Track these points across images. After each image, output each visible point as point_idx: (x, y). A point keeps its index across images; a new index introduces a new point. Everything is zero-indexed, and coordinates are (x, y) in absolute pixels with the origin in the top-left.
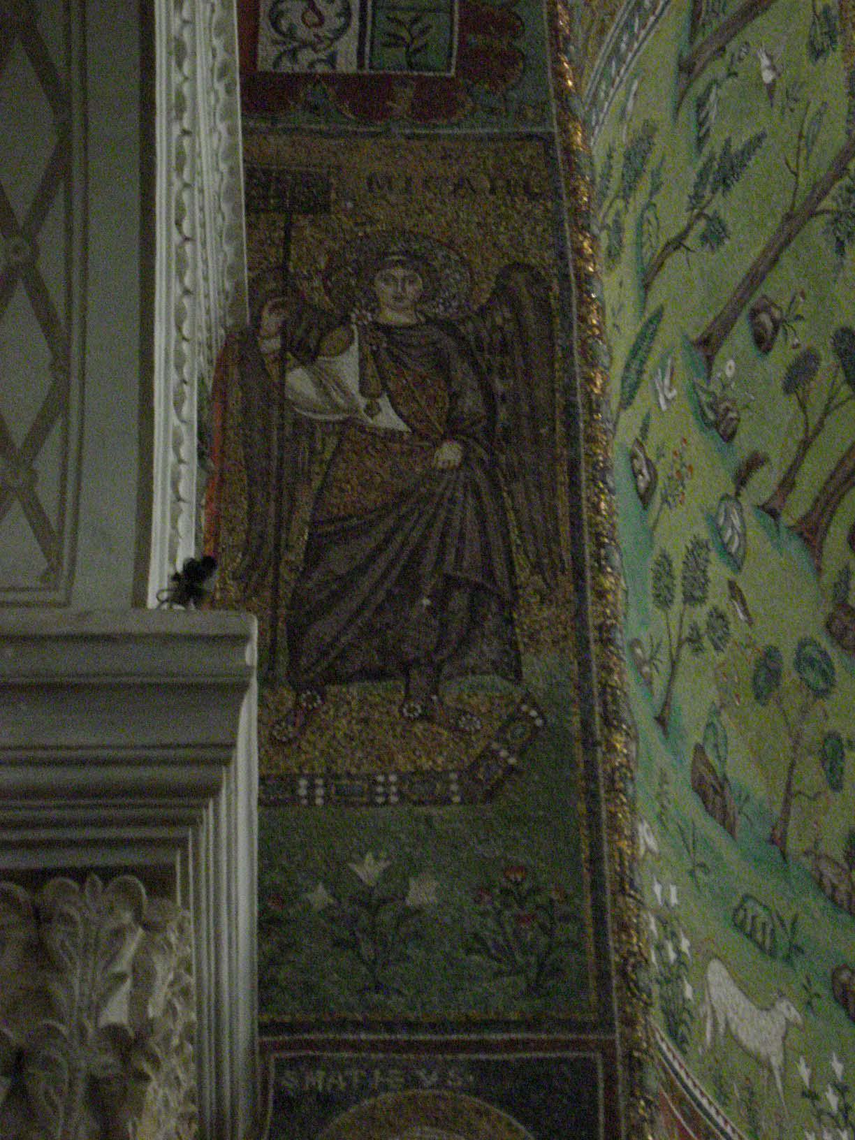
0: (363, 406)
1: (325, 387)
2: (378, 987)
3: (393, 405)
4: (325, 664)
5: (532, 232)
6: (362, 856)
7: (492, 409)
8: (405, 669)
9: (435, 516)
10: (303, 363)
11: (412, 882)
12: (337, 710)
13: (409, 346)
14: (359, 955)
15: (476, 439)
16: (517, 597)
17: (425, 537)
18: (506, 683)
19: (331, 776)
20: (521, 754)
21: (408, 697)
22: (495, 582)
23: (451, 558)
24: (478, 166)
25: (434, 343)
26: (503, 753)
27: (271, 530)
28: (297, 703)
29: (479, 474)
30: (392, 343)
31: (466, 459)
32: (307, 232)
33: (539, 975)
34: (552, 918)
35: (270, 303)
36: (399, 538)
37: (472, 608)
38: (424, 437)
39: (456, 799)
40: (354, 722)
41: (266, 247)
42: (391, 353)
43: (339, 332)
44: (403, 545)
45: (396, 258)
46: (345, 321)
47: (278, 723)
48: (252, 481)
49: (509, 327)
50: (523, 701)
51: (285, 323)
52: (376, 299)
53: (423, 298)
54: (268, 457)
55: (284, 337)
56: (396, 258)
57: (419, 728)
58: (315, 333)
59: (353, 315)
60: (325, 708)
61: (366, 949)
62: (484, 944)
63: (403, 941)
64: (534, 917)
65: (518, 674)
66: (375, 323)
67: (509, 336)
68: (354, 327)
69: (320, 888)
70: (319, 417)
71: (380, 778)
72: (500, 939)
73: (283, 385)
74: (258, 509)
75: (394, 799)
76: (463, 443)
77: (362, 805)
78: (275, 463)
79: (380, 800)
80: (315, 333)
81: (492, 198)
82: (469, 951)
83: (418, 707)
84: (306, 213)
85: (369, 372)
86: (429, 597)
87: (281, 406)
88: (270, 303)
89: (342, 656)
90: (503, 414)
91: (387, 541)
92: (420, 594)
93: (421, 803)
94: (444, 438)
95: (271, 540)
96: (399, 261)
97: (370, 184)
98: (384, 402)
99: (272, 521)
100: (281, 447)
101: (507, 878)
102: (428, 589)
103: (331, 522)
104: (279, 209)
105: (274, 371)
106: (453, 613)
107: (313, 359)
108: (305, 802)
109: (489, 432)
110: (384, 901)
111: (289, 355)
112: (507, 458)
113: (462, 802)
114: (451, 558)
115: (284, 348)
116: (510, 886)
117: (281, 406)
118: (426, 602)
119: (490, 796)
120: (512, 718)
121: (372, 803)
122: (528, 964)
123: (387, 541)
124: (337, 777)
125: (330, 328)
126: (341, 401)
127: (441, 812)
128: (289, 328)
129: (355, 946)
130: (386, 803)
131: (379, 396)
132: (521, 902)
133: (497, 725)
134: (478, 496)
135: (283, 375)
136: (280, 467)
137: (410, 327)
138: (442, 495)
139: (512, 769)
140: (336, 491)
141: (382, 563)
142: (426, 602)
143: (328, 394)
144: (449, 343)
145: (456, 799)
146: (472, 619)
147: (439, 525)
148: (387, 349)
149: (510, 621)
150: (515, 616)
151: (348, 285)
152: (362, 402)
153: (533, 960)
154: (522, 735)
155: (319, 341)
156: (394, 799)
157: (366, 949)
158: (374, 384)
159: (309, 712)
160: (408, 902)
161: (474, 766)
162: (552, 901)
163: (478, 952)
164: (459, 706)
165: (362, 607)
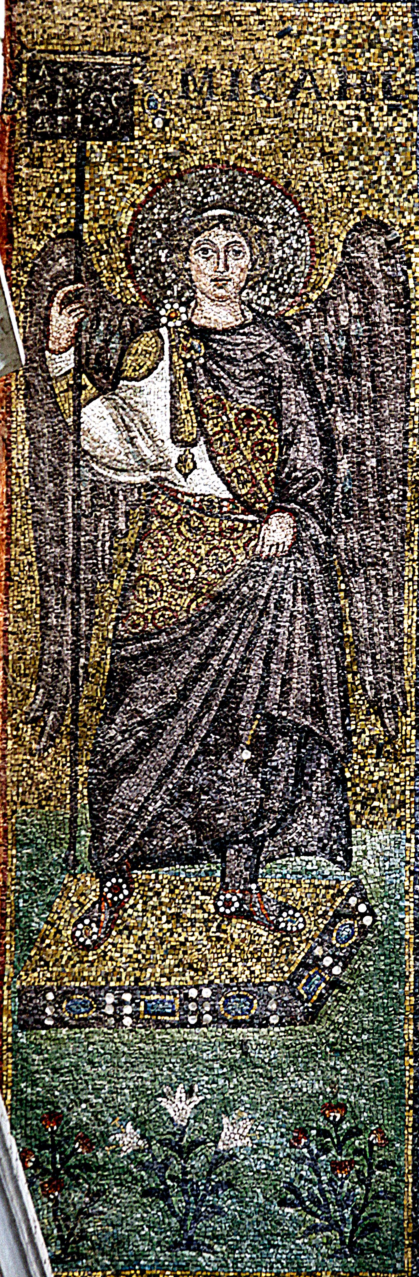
0: (175, 461)
1: (128, 429)
2: (190, 1244)
3: (211, 458)
4: (132, 841)
5: (390, 166)
6: (174, 1088)
7: (330, 461)
8: (221, 848)
9: (257, 631)
10: (102, 391)
11: (225, 1120)
12: (145, 903)
13: (231, 361)
14: (171, 1206)
15: (311, 509)
16: (350, 748)
17: (246, 661)
18: (334, 867)
19: (138, 988)
20: (346, 961)
21: (225, 887)
22: (326, 725)
23: (275, 692)
24: (324, 47)
25: (261, 356)
26: (328, 961)
27: (67, 652)
28: (102, 898)
29: (313, 566)
30: (211, 358)
31: (297, 538)
32: (105, 171)
33: (352, 1232)
34: (370, 1166)
35: (60, 294)
36: (215, 662)
37: (300, 764)
38: (249, 509)
39: (274, 1020)
40: (164, 918)
41: (54, 199)
42: (208, 372)
43: (146, 341)
44: (220, 673)
45: (217, 212)
46: (153, 323)
47: (81, 920)
48: (44, 576)
49: (357, 328)
50: (352, 892)
51: (78, 326)
52: (190, 286)
53: (252, 283)
54: (62, 542)
55: (78, 352)
56: (217, 212)
57: (236, 929)
58: (115, 345)
59: (163, 312)
60: (132, 902)
61: (178, 1202)
62: (298, 1196)
63: (214, 1191)
64: (352, 1163)
65: (348, 855)
66: (189, 323)
67: (355, 342)
68: (164, 331)
69: (129, 1127)
70: (123, 478)
71: (193, 993)
72: (316, 1192)
73: (77, 424)
74: (52, 621)
75: (208, 1018)
76: (292, 513)
77: (173, 1026)
78: (70, 553)
79: (192, 1020)
80: (115, 345)
81: (341, 105)
82: (283, 1203)
83: (234, 899)
84: (104, 136)
85: (183, 406)
86: (248, 747)
87: (76, 463)
88: (60, 294)
89: (149, 833)
90: (344, 466)
91: (203, 667)
92: (236, 742)
93: (236, 1024)
94: (272, 510)
95: (69, 665)
96: (222, 218)
97: (184, 82)
98: (200, 451)
99: (69, 638)
100: (77, 527)
101: (327, 1118)
102: (246, 735)
103: (138, 638)
104: (69, 130)
105: (67, 407)
106: (275, 768)
107: (115, 386)
108: (112, 1021)
109: (327, 499)
110: (195, 1144)
111: (85, 380)
112: (347, 541)
113: (280, 1024)
114: (275, 692)
115: (79, 368)
116: (330, 1128)
117: (76, 463)
118: (247, 755)
119: (311, 1017)
120: (338, 915)
121: (183, 1024)
122: (344, 1220)
123: (203, 667)
124: (147, 990)
125: (136, 333)
126: (148, 453)
127: (257, 1036)
128: (85, 338)
129: (165, 1196)
130: (199, 1024)
131: (194, 444)
132: (339, 1147)
133: (323, 923)
134: (309, 598)
135: (77, 412)
136: (76, 557)
137: (233, 331)
138: (269, 596)
139: (334, 984)
140: (142, 595)
141: (195, 702)
142: (247, 755)
143: (131, 440)
144: (281, 355)
145: (274, 1020)
146: (298, 779)
147: (262, 641)
148: (205, 364)
149: (341, 781)
150: (348, 775)
151: (158, 262)
152: (174, 452)
153: (347, 1213)
154: (350, 937)
155: (123, 353)
156: (208, 1018)
157: (178, 1202)
158: (190, 427)
159: (114, 903)
160: (221, 1146)
161: (295, 978)
162: (371, 1144)
163: (292, 1205)
164: (280, 899)
165: (173, 763)
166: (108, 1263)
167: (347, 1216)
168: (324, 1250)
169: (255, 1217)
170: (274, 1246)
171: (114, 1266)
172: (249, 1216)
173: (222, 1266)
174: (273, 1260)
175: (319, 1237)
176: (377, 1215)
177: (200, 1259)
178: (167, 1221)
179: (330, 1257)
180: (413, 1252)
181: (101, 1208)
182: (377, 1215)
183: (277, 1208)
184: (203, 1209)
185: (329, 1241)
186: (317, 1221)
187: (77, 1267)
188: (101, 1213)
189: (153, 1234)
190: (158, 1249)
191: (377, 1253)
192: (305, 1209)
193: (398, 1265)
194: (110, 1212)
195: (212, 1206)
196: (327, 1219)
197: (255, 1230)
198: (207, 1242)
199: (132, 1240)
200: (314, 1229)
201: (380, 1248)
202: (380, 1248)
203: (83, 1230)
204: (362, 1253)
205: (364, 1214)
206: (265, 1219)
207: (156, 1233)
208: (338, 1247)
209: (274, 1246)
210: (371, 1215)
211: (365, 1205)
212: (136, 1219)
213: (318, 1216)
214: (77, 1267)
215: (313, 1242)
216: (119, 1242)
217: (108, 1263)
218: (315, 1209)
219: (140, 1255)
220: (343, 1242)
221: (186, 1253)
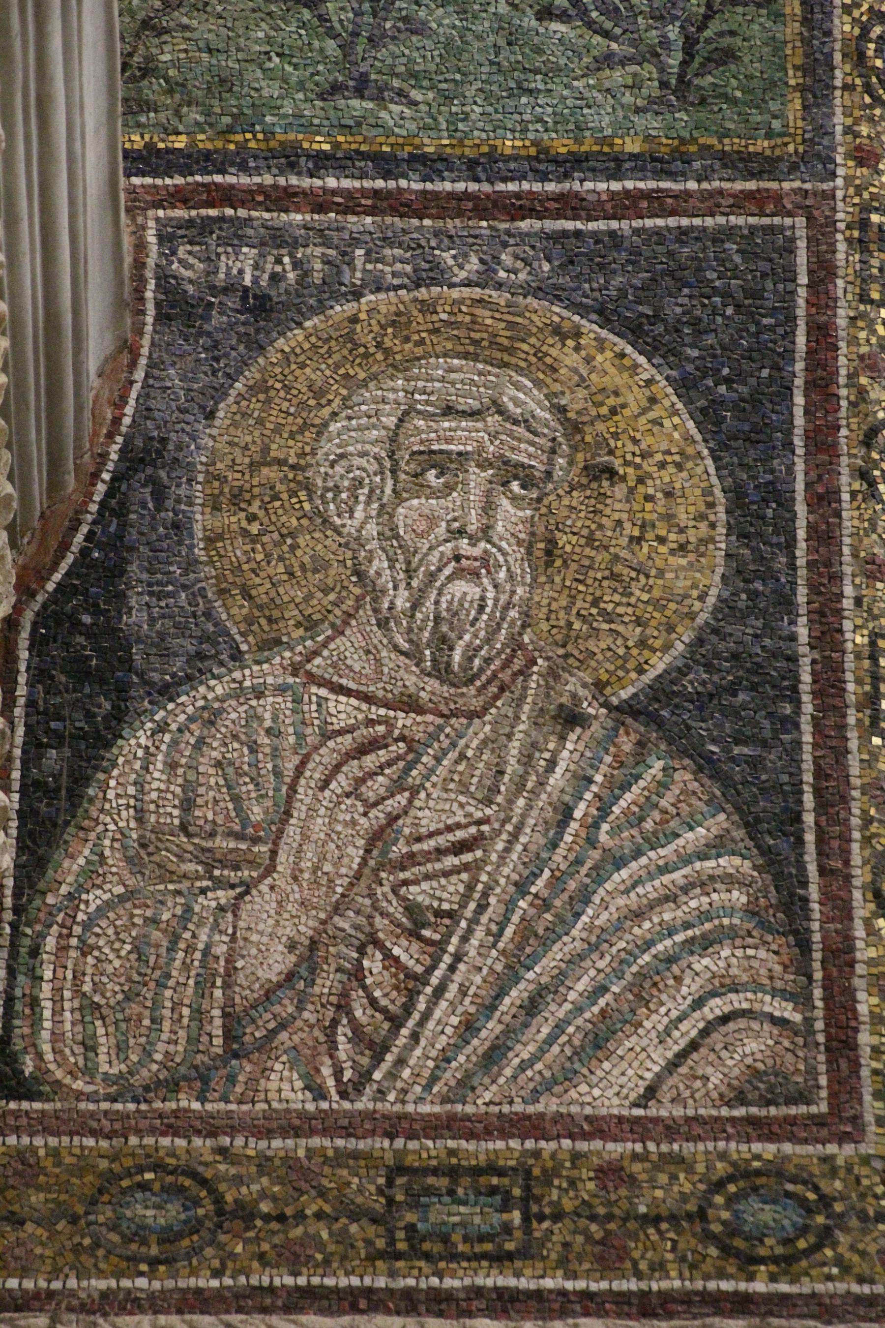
33: (684, 63)
122: (665, 43)
153: (673, 32)
166: (200, 119)
167: (672, 36)
168: (628, 98)
169: (491, 38)
170: (530, 92)
171: (211, 125)
172: (479, 38)
173: (426, 127)
174: (527, 117)
175: (617, 76)
176: (732, 33)
177: (383, 114)
178: (316, 44)
179: (638, 110)
180: (804, 99)
181: (185, 20)
182: (732, 33)
183: (534, 23)
184: (388, 25)
185: (635, 86)
186: (614, 46)
187: (139, 125)
188: (186, 28)
189: (289, 68)
190: (300, 96)
191: (734, 102)
192: (590, 25)
193: (776, 124)
194: (202, 27)
195: (405, 19)
196: (633, 43)
197: (491, 63)
198: (396, 83)
199: (247, 76)
200: (607, 60)
201: (738, 94)
202: (738, 94)
203: (150, 59)
204: (703, 101)
205: (708, 33)
206: (509, 44)
207: (296, 67)
208: (656, 93)
209: (530, 92)
210: (721, 34)
211: (707, 18)
212: (257, 41)
213: (615, 39)
214: (139, 125)
215: (607, 85)
216: (222, 81)
217: (200, 119)
218: (608, 25)
219: (262, 107)
220: (664, 85)
221: (355, 103)
